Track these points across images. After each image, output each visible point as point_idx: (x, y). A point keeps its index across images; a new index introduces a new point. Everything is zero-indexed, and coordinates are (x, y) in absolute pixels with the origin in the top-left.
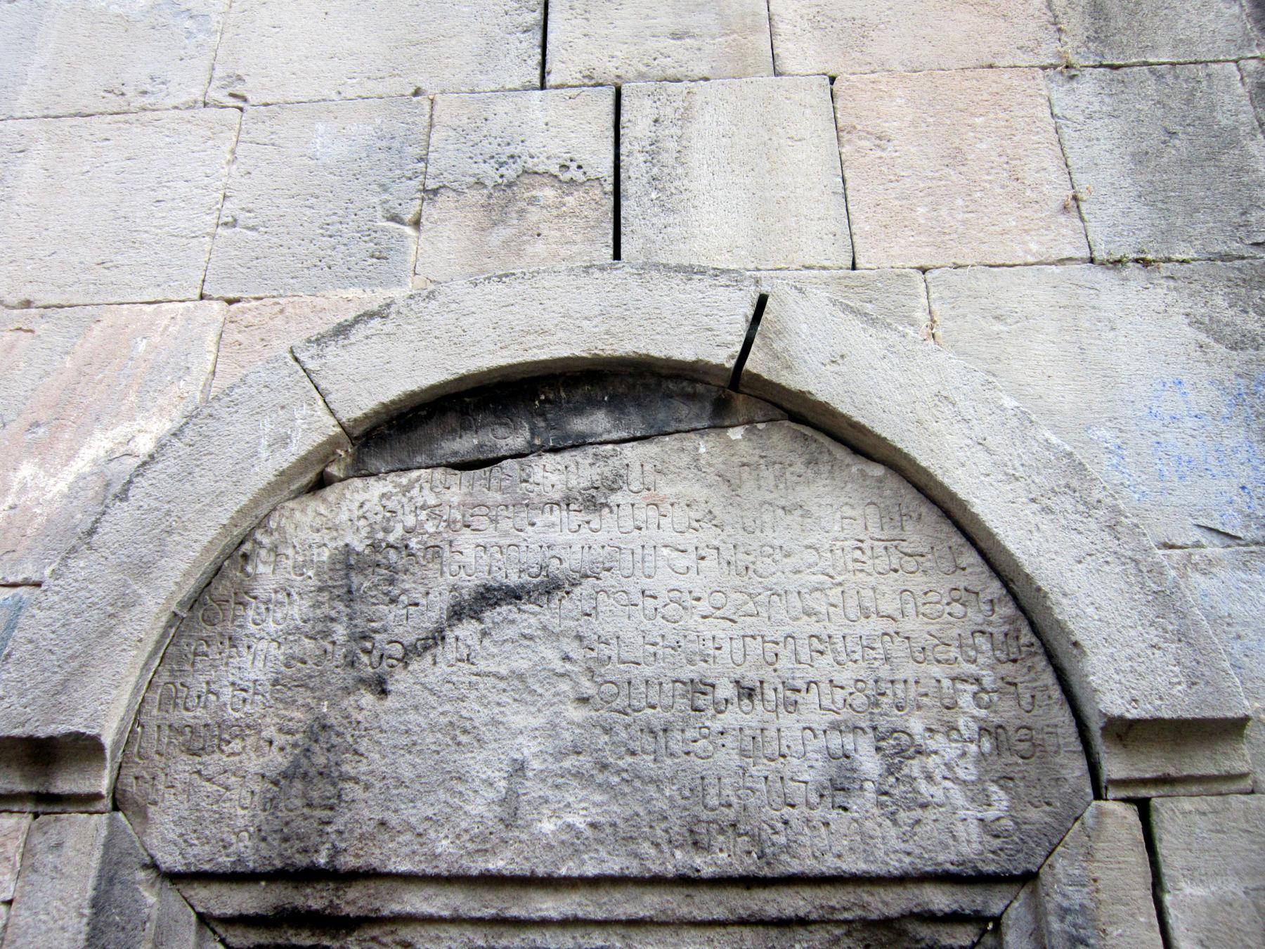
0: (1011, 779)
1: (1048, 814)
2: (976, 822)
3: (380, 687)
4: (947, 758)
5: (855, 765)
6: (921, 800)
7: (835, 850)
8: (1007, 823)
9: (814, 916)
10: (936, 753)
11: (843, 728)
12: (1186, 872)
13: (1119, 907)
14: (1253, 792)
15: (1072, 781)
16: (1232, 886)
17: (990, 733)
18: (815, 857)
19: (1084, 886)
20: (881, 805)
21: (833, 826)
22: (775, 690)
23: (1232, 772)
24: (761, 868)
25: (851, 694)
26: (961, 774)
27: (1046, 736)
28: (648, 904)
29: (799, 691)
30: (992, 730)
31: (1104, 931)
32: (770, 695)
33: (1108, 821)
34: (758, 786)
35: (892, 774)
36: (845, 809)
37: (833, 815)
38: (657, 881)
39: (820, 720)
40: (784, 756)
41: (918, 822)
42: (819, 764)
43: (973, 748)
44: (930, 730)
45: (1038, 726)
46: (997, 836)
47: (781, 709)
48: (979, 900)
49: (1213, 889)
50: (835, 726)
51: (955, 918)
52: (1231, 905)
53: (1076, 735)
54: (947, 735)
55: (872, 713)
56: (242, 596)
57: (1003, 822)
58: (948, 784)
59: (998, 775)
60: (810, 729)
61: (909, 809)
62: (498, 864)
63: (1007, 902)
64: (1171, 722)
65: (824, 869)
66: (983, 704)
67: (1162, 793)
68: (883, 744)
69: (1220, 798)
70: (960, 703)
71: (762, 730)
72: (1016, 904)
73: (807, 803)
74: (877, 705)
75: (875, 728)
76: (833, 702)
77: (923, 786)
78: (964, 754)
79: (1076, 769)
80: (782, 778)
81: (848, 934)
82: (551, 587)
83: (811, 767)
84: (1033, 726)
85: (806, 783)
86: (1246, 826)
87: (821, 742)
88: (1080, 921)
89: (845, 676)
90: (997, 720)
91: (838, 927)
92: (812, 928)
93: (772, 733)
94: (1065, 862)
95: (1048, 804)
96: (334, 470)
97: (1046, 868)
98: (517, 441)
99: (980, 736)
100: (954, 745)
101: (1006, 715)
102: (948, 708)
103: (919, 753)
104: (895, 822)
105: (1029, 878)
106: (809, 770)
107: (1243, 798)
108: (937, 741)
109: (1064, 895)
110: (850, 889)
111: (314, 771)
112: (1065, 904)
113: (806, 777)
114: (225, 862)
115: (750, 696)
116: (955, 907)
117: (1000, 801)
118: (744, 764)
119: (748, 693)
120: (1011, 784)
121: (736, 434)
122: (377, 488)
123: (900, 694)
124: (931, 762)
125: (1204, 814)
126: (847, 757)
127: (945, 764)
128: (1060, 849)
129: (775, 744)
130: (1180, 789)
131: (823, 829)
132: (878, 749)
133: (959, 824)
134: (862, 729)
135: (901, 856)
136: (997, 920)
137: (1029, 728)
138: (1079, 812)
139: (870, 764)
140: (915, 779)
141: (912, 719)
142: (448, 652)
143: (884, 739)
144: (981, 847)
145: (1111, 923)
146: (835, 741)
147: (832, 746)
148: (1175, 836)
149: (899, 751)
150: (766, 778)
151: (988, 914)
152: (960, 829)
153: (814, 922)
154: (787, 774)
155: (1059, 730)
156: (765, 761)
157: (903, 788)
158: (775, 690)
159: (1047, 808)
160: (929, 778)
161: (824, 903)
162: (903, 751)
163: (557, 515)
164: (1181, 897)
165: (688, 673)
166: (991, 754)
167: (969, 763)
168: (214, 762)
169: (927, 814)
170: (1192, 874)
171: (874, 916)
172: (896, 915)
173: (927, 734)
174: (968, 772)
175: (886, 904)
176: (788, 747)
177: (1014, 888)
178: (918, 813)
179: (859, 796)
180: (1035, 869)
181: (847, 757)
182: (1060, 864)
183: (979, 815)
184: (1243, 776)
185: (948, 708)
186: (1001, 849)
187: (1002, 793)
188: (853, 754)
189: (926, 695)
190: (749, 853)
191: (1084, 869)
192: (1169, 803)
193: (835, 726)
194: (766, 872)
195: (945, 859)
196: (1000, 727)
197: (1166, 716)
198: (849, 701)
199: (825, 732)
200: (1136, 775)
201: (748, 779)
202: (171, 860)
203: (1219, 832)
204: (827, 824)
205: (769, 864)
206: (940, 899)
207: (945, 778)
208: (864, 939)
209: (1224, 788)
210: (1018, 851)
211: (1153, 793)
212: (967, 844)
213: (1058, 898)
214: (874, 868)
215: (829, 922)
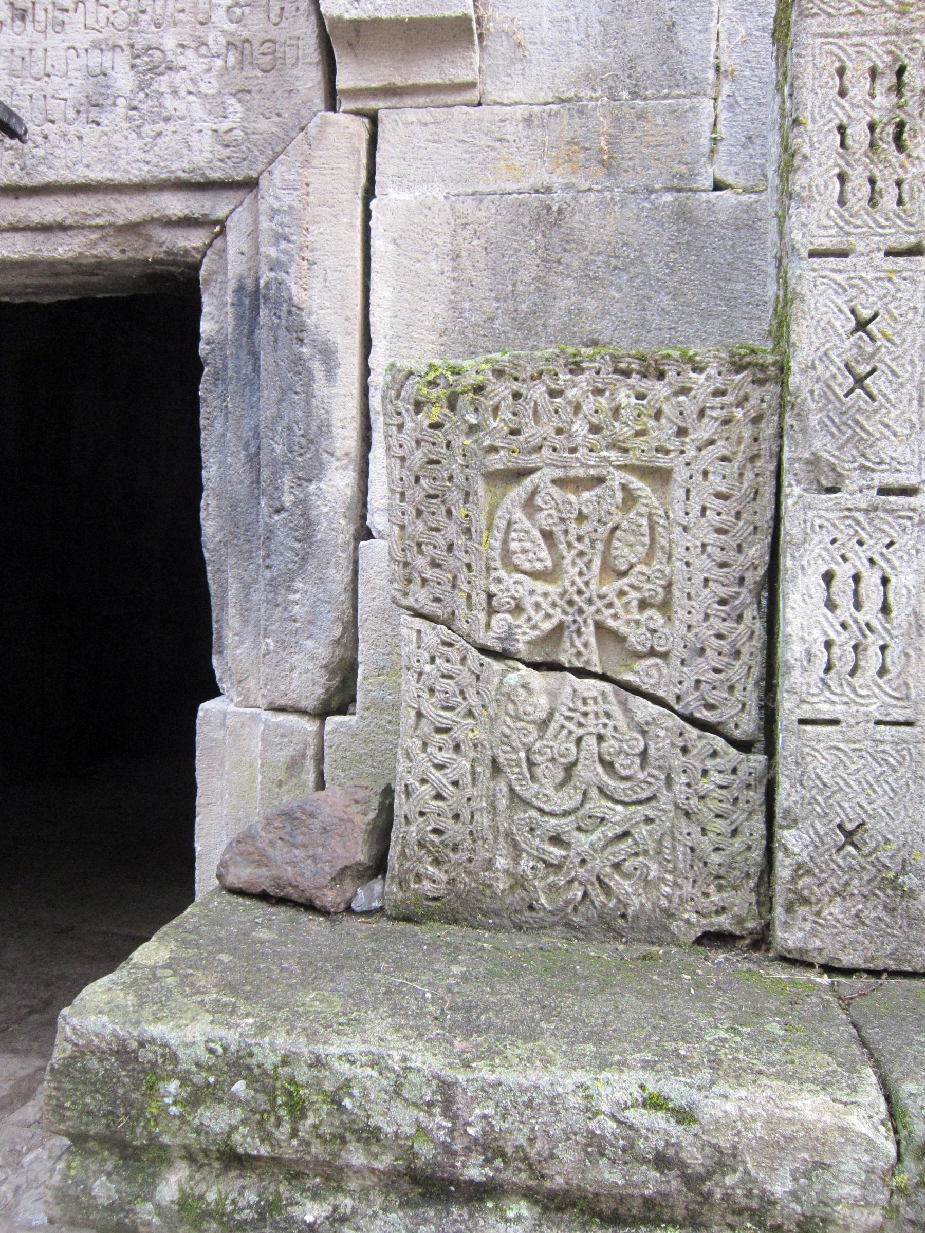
0: (249, 92)
1: (277, 124)
2: (210, 133)
4: (193, 72)
5: (110, 82)
6: (165, 114)
7: (85, 162)
8: (238, 133)
9: (69, 222)
10: (184, 68)
11: (103, 47)
12: (395, 179)
13: (325, 208)
14: (480, 104)
15: (303, 92)
16: (435, 192)
17: (236, 47)
18: (68, 167)
19: (296, 189)
20: (129, 119)
21: (85, 140)
22: (46, 10)
23: (457, 81)
24: (21, 178)
25: (114, 12)
26: (204, 88)
27: (287, 49)
29: (67, 11)
30: (239, 44)
31: (307, 229)
32: (41, 15)
33: (331, 130)
34: (24, 104)
35: (143, 90)
36: (98, 124)
37: (86, 130)
39: (83, 39)
40: (48, 76)
41: (159, 134)
42: (77, 82)
43: (219, 62)
44: (183, 46)
45: (282, 39)
46: (227, 146)
47: (50, 29)
48: (208, 205)
49: (417, 194)
51: (188, 222)
52: (430, 208)
53: (315, 46)
54: (197, 49)
55: (131, 31)
57: (235, 132)
58: (191, 98)
59: (237, 88)
60: (74, 48)
61: (154, 122)
63: (232, 207)
64: (390, 21)
65: (74, 178)
66: (235, 18)
67: (389, 104)
68: (138, 61)
69: (446, 110)
70: (214, 19)
71: (31, 50)
72: (240, 209)
73: (65, 120)
74: (136, 22)
75: (132, 46)
76: (97, 21)
77: (169, 102)
78: (209, 70)
79: (310, 79)
80: (45, 96)
81: (103, 238)
83: (71, 85)
84: (277, 39)
85: (65, 100)
86: (464, 137)
87: (82, 61)
88: (286, 220)
90: (245, 34)
91: (93, 232)
92: (71, 233)
93: (39, 53)
94: (283, 169)
95: (279, 115)
97: (265, 174)
99: (227, 50)
100: (201, 60)
101: (254, 28)
102: (202, 24)
103: (170, 69)
104: (139, 135)
105: (250, 185)
106: (71, 88)
107: (465, 109)
108: (189, 59)
109: (277, 198)
110: (101, 197)
112: (276, 205)
113: (66, 95)
115: (23, 18)
116: (187, 211)
118: (12, 84)
120: (248, 97)
123: (159, 10)
124: (178, 77)
125: (426, 125)
126: (105, 75)
127: (191, 79)
128: (282, 156)
129: (41, 64)
130: (408, 101)
131: (77, 142)
132: (133, 67)
133: (196, 135)
134: (120, 47)
135: (141, 165)
136: (222, 223)
137: (273, 42)
138: (305, 122)
139: (124, 80)
140: (162, 94)
141: (166, 36)
143: (138, 56)
144: (211, 156)
145: (315, 223)
146: (95, 59)
147: (91, 64)
148: (394, 147)
149: (152, 67)
150: (31, 96)
151: (213, 217)
152: (195, 140)
153: (71, 227)
154: (49, 93)
155: (301, 43)
156: (32, 80)
157: (150, 103)
158: (46, 10)
159: (276, 119)
160: (175, 93)
161: (78, 209)
162: (156, 67)
164: (385, 201)
166: (233, 69)
167: (212, 76)
169: (167, 127)
170: (400, 180)
171: (120, 222)
172: (139, 220)
173: (179, 50)
175: (130, 210)
176: (53, 66)
177: (240, 195)
178: (161, 126)
179: (111, 112)
180: (255, 175)
181: (105, 75)
182: (278, 169)
183: (214, 127)
184: (472, 85)
185: (202, 24)
186: (229, 158)
187: (238, 106)
188: (109, 71)
189: (183, 11)
190: (13, 165)
191: (300, 174)
192: (394, 114)
193: (96, 45)
194: (26, 181)
195: (179, 168)
196: (247, 41)
197: (384, 16)
198: (112, 19)
199: (87, 50)
200: (363, 84)
201: (15, 97)
203: (435, 142)
204: (80, 138)
205: (28, 174)
206: (175, 205)
207: (190, 93)
208: (118, 245)
209: (450, 99)
210: (244, 159)
211: (381, 104)
212: (201, 155)
213: (271, 200)
214: (118, 177)
215: (83, 227)
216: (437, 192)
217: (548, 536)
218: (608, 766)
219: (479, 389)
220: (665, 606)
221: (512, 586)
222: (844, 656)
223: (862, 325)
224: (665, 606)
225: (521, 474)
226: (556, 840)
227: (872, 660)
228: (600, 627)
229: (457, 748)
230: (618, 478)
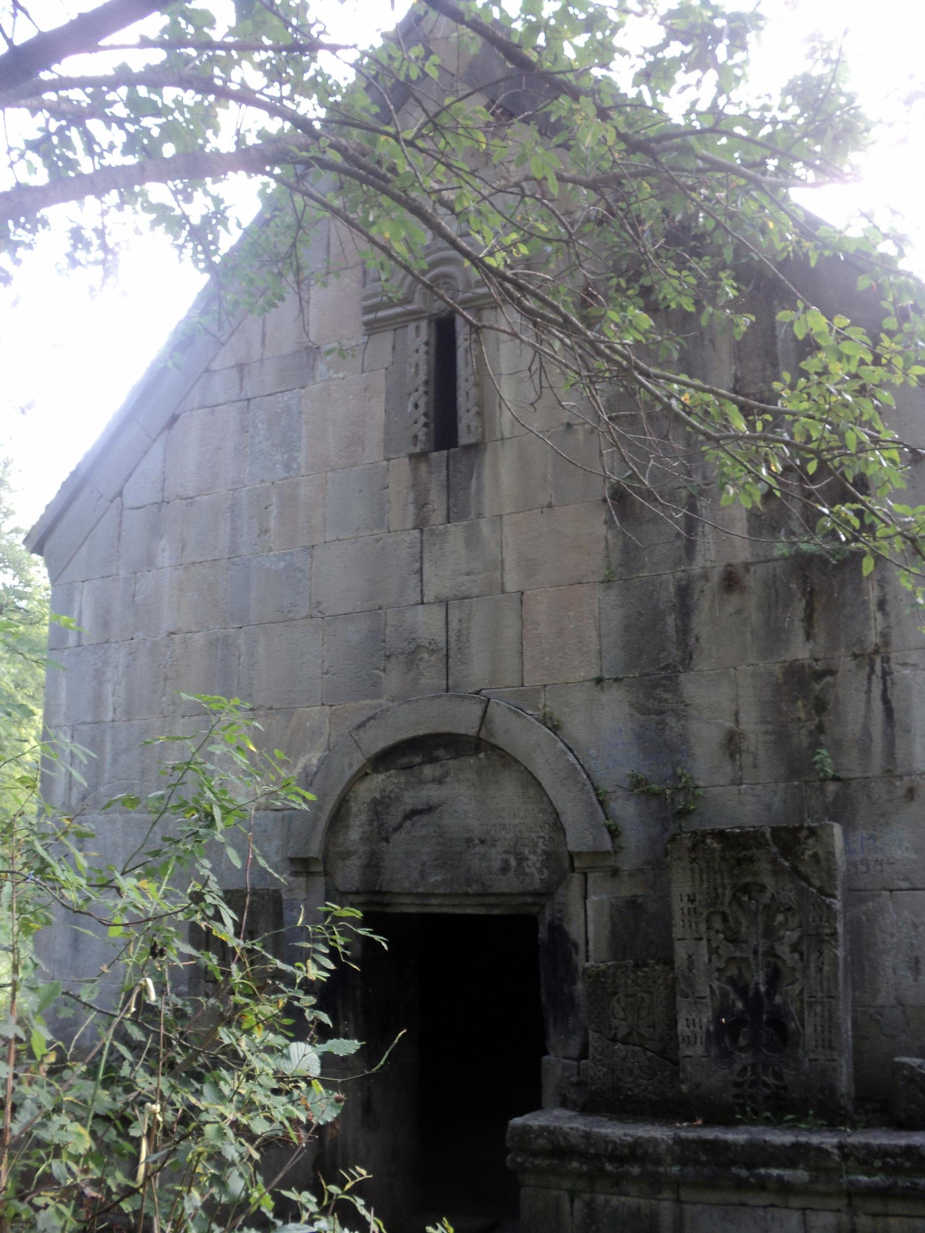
3: (387, 840)
28: (457, 901)
38: (458, 895)
50: (505, 852)
56: (348, 812)
62: (420, 890)
79: (566, 864)
82: (429, 809)
89: (508, 837)
96: (369, 771)
98: (418, 760)
106: (497, 864)
111: (373, 865)
114: (354, 889)
117: (546, 873)
119: (482, 842)
121: (482, 755)
122: (382, 776)
139: (513, 863)
142: (403, 831)
163: (430, 786)
165: (466, 836)
168: (348, 862)
170: (595, 894)
174: (538, 865)
202: (341, 889)
216: (605, 897)
217: (624, 1010)
218: (641, 1069)
219: (604, 972)
220: (654, 1027)
221: (615, 1022)
222: (692, 1039)
223: (690, 956)
224: (654, 1027)
225: (615, 993)
226: (629, 1089)
227: (699, 1040)
228: (638, 1034)
229: (603, 1065)
230: (639, 994)
